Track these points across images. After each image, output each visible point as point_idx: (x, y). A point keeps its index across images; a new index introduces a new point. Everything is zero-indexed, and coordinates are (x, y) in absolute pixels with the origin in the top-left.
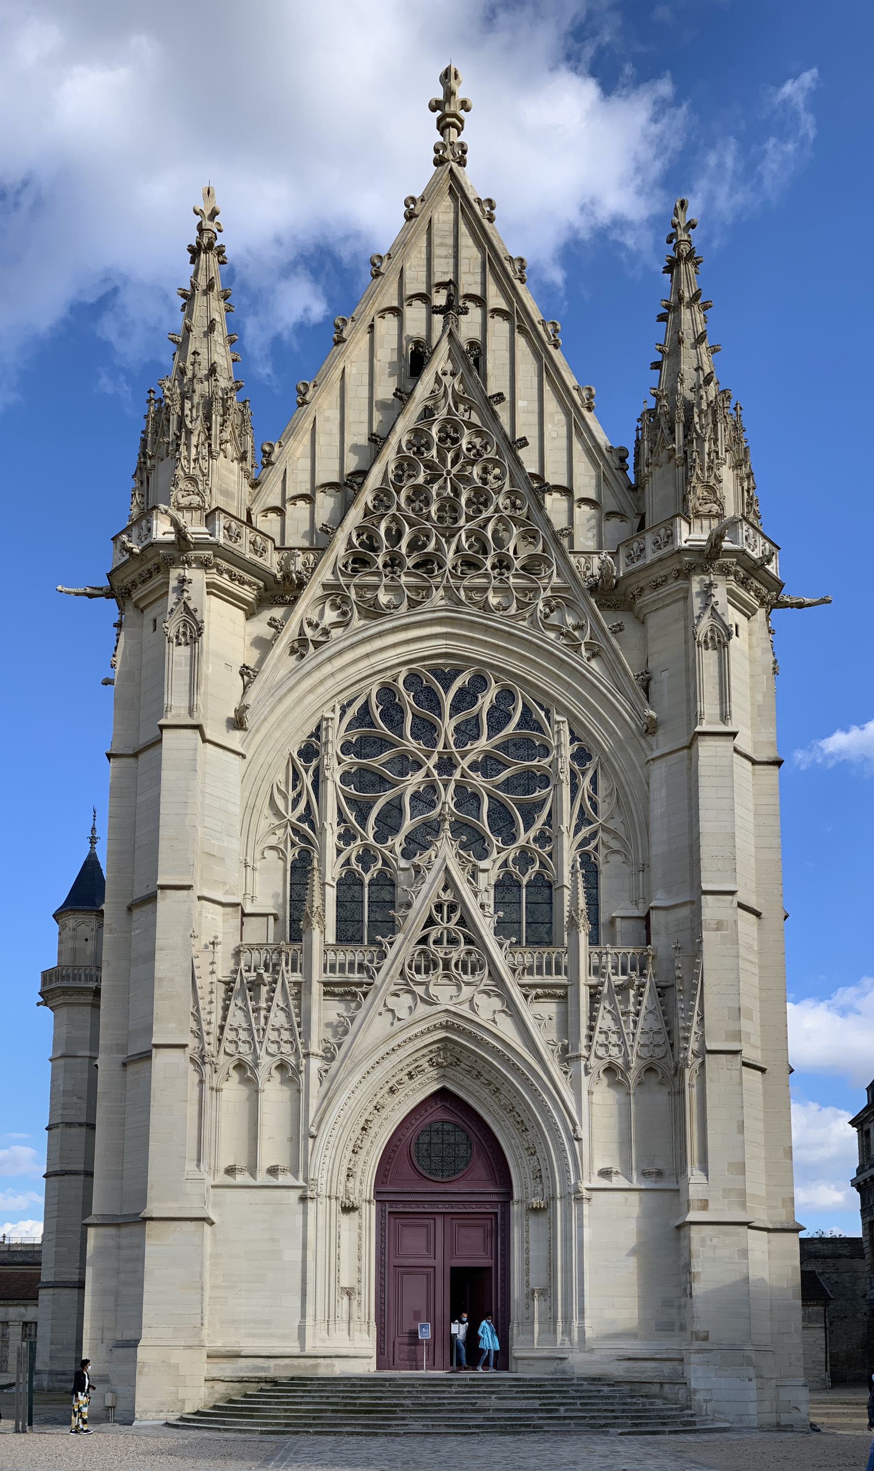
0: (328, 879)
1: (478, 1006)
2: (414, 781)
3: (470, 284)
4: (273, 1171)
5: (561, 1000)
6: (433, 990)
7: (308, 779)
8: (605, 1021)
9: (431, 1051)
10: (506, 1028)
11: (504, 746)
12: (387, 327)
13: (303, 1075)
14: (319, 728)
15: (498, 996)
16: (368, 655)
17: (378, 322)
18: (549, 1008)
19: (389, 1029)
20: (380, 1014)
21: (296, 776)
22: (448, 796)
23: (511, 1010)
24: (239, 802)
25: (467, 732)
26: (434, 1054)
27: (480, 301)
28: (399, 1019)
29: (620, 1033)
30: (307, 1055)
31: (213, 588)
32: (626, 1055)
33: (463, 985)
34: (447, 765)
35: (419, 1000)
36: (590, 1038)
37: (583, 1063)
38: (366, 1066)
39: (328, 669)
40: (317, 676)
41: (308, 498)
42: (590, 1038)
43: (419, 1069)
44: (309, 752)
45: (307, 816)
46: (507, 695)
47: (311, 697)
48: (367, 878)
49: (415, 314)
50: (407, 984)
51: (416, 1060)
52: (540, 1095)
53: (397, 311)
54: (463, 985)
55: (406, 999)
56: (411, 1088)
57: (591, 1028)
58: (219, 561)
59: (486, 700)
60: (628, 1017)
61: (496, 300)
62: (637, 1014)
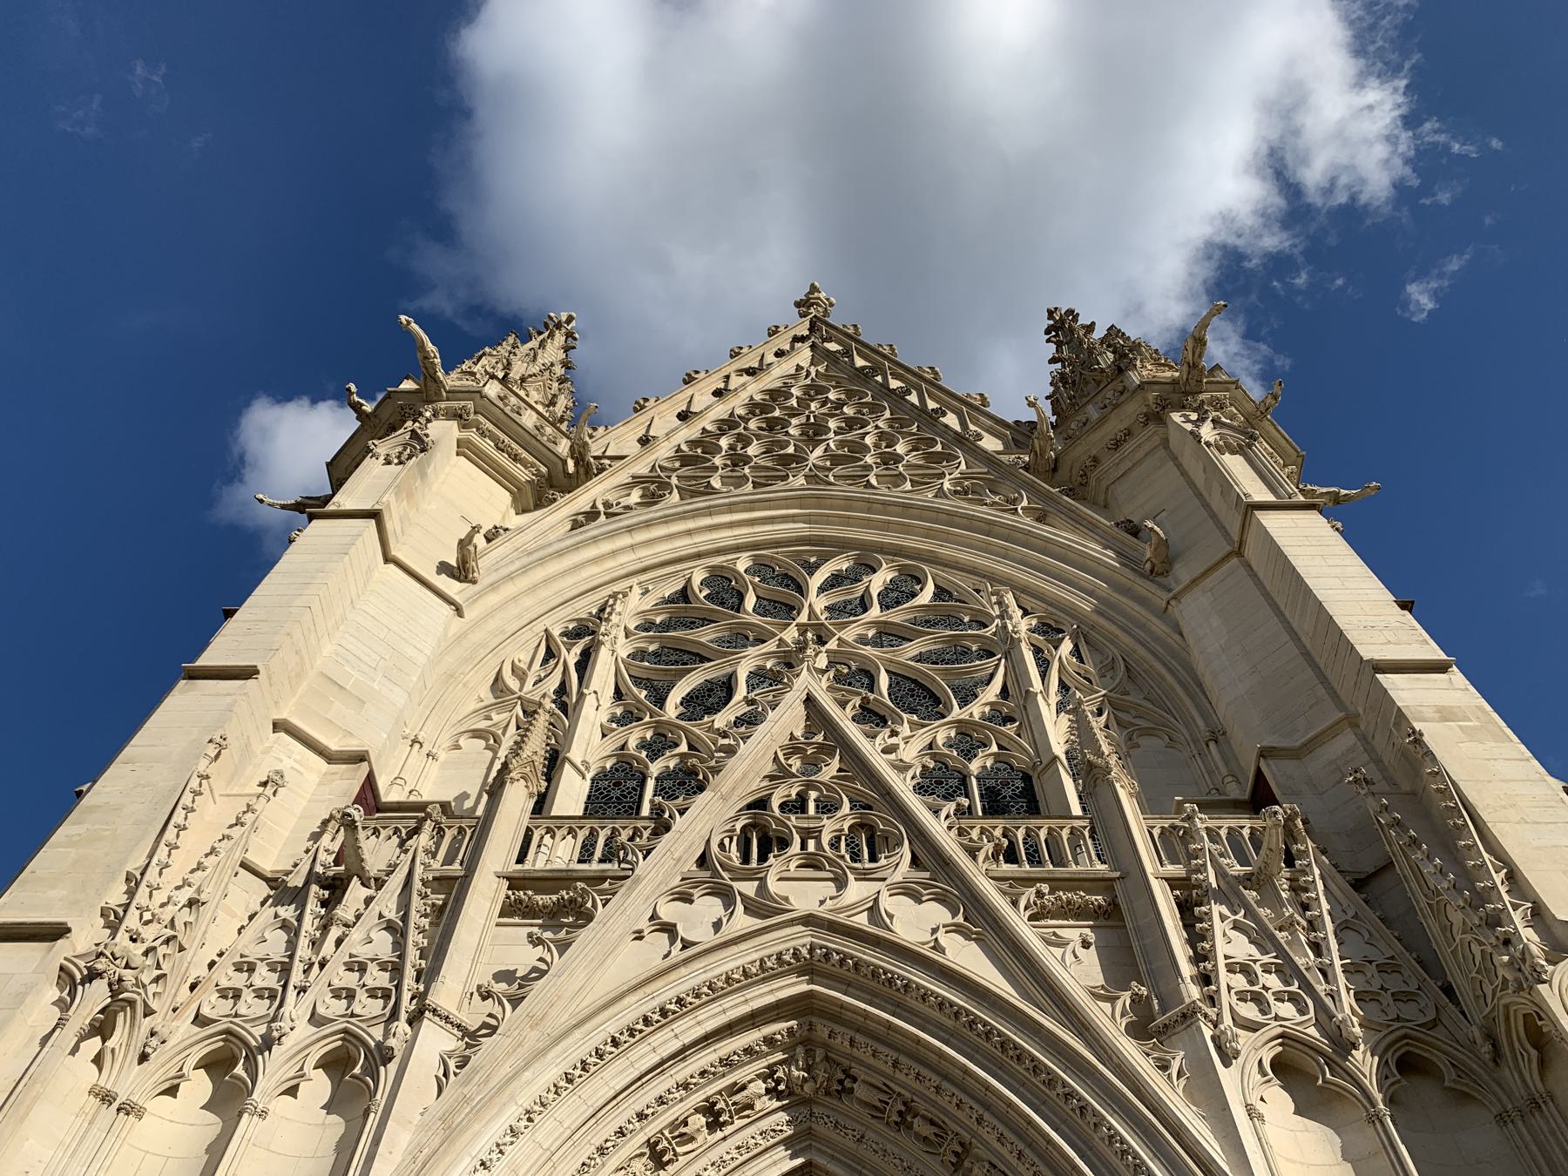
0: (576, 753)
1: (891, 917)
5: (1101, 922)
6: (774, 886)
7: (572, 657)
8: (1230, 944)
9: (769, 1041)
13: (393, 1067)
14: (602, 610)
15: (941, 899)
16: (689, 533)
17: (733, 376)
19: (658, 963)
20: (639, 936)
21: (550, 654)
24: (428, 652)
26: (779, 1056)
28: (686, 945)
29: (1286, 970)
30: (415, 1019)
31: (463, 448)
32: (1324, 1017)
33: (851, 877)
35: (740, 908)
36: (1205, 979)
37: (1208, 1033)
38: (580, 1046)
39: (626, 540)
40: (606, 547)
42: (1205, 979)
43: (736, 1098)
47: (594, 569)
48: (655, 768)
50: (716, 874)
51: (727, 1063)
52: (1099, 1122)
54: (851, 877)
55: (711, 907)
56: (714, 1155)
57: (1199, 958)
58: (481, 418)
60: (1293, 933)
62: (1312, 925)
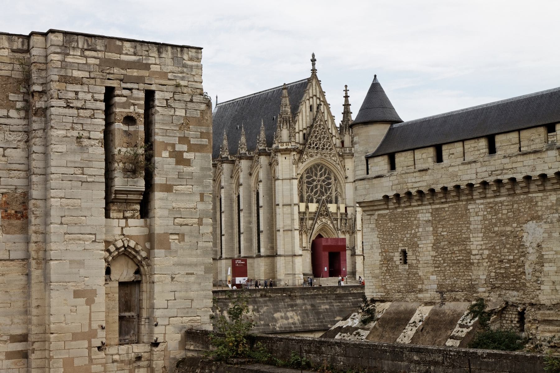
2: (315, 183)
3: (318, 96)
4: (305, 247)
10: (331, 225)
11: (326, 178)
12: (307, 102)
18: (335, 222)
22: (319, 187)
23: (332, 223)
25: (321, 175)
27: (319, 99)
34: (319, 181)
41: (299, 133)
44: (301, 178)
45: (302, 189)
46: (326, 169)
49: (311, 100)
53: (309, 100)
59: (323, 170)
61: (322, 99)
